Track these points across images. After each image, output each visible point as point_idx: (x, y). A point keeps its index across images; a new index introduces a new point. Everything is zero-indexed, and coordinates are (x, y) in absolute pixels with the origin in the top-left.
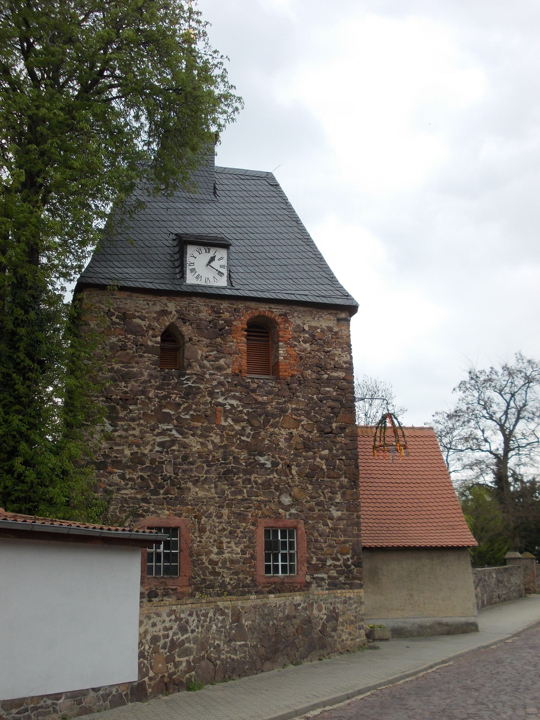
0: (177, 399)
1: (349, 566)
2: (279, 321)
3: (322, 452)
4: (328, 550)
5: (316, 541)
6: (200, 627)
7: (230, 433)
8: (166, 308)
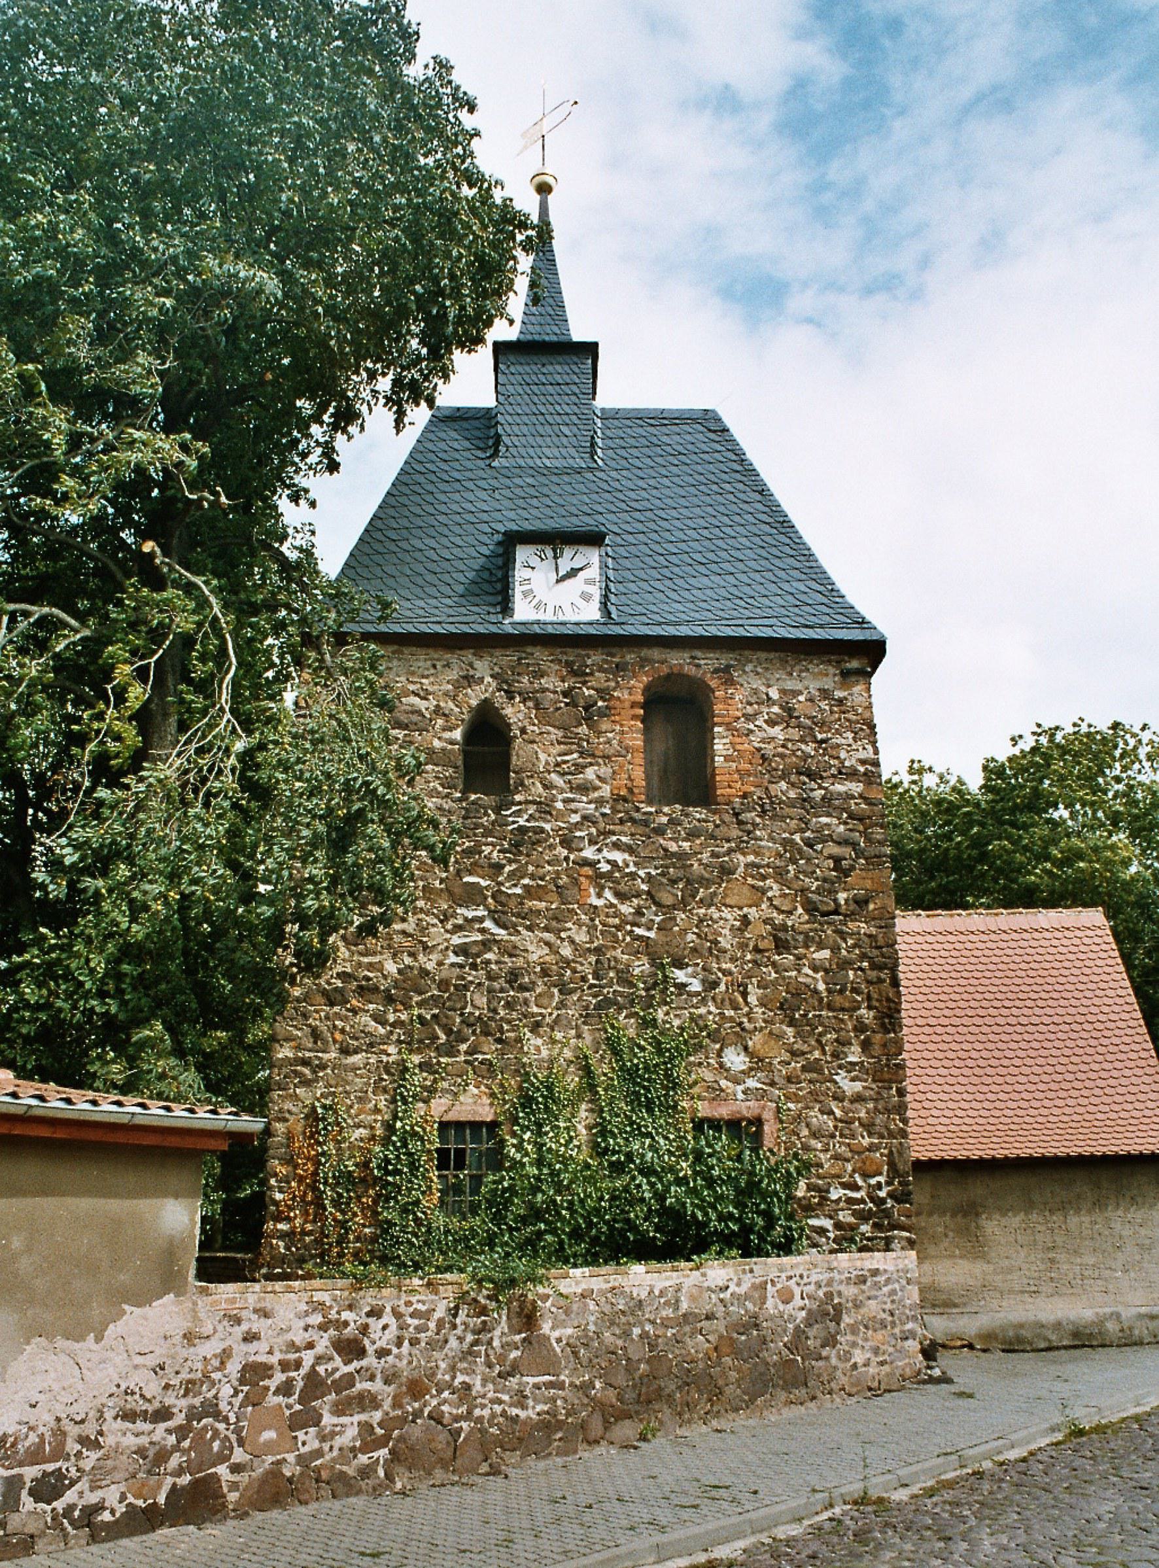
0: (495, 854)
1: (883, 1201)
2: (713, 684)
3: (815, 956)
4: (833, 1165)
5: (806, 1148)
6: (406, 1343)
7: (611, 921)
8: (471, 673)
